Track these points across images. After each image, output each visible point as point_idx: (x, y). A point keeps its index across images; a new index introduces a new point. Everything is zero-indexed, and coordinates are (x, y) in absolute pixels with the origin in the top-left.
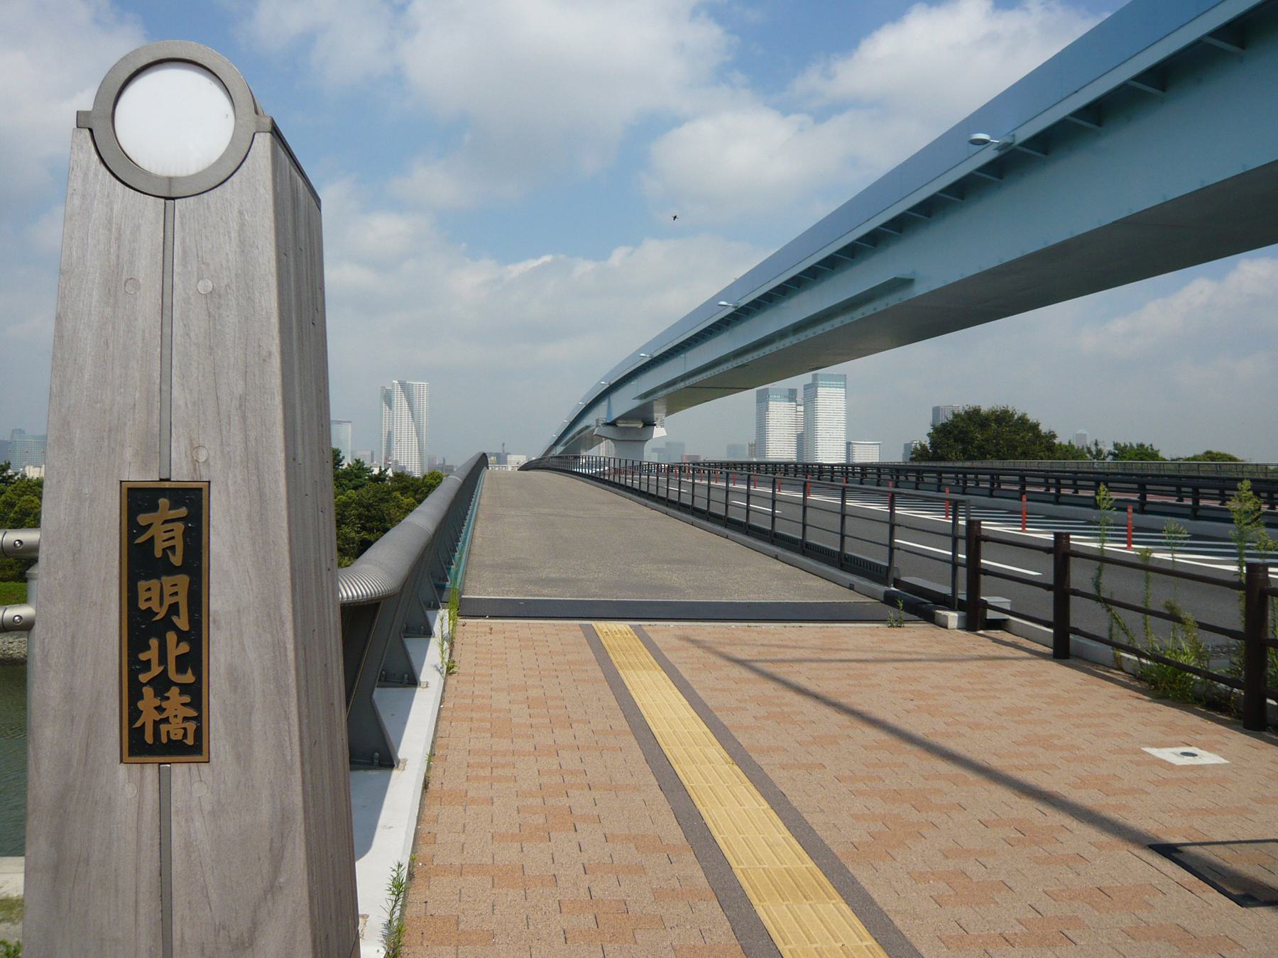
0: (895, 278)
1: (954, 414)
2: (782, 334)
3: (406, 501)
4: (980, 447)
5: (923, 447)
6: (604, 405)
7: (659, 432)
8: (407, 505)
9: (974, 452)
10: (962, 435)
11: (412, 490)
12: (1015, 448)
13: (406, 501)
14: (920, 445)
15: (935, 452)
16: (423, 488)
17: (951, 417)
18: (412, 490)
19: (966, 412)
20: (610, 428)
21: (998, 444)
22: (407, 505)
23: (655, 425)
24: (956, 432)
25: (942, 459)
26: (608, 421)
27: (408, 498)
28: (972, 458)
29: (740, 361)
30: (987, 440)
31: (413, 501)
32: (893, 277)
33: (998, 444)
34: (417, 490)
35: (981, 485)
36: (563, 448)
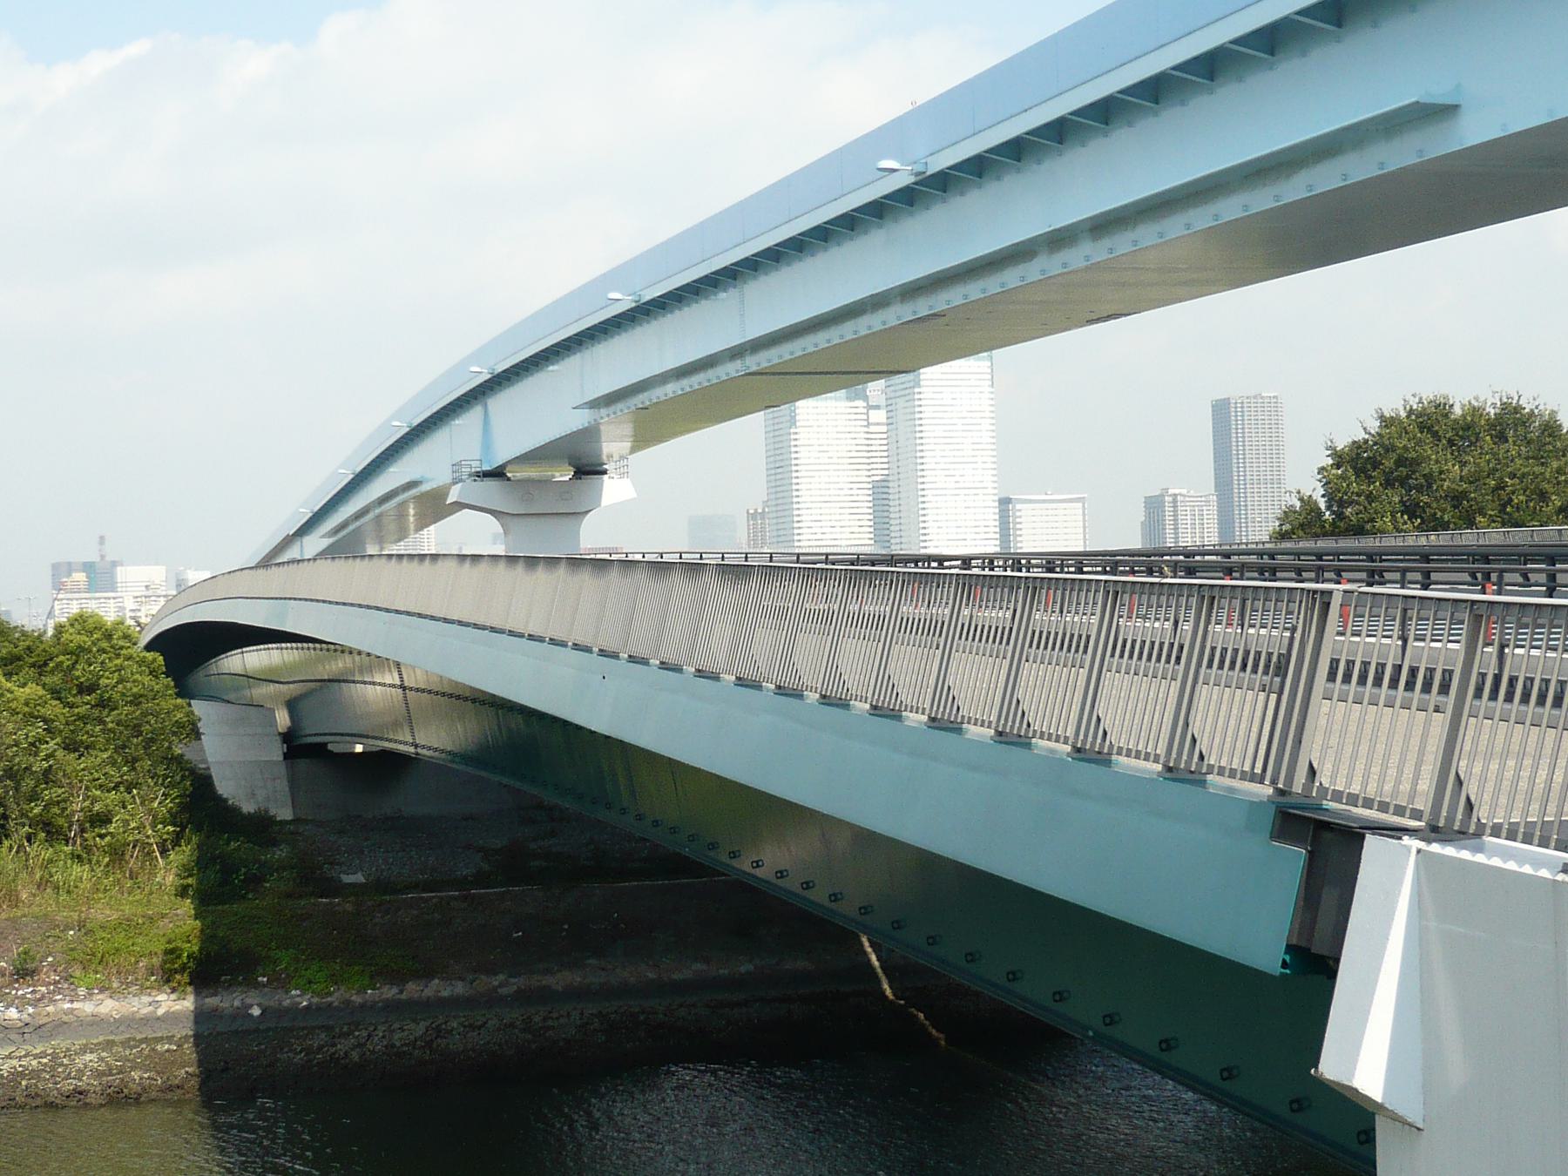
0: (1418, 102)
1: (1382, 418)
2: (1058, 240)
3: (22, 693)
4: (1457, 498)
5: (1308, 503)
6: (468, 423)
7: (614, 489)
8: (27, 704)
9: (1444, 511)
10: (1404, 471)
11: (33, 665)
12: (1543, 496)
13: (22, 693)
14: (1301, 499)
15: (1340, 516)
16: (61, 658)
17: (1374, 426)
18: (33, 665)
19: (1411, 412)
20: (491, 484)
21: (1501, 486)
22: (27, 704)
23: (605, 472)
24: (1387, 464)
25: (1359, 531)
26: (486, 467)
27: (24, 685)
28: (1437, 525)
29: (922, 307)
30: (1474, 479)
31: (41, 692)
32: (1413, 100)
33: (1501, 486)
34: (46, 664)
35: (1544, 588)
36: (326, 542)
